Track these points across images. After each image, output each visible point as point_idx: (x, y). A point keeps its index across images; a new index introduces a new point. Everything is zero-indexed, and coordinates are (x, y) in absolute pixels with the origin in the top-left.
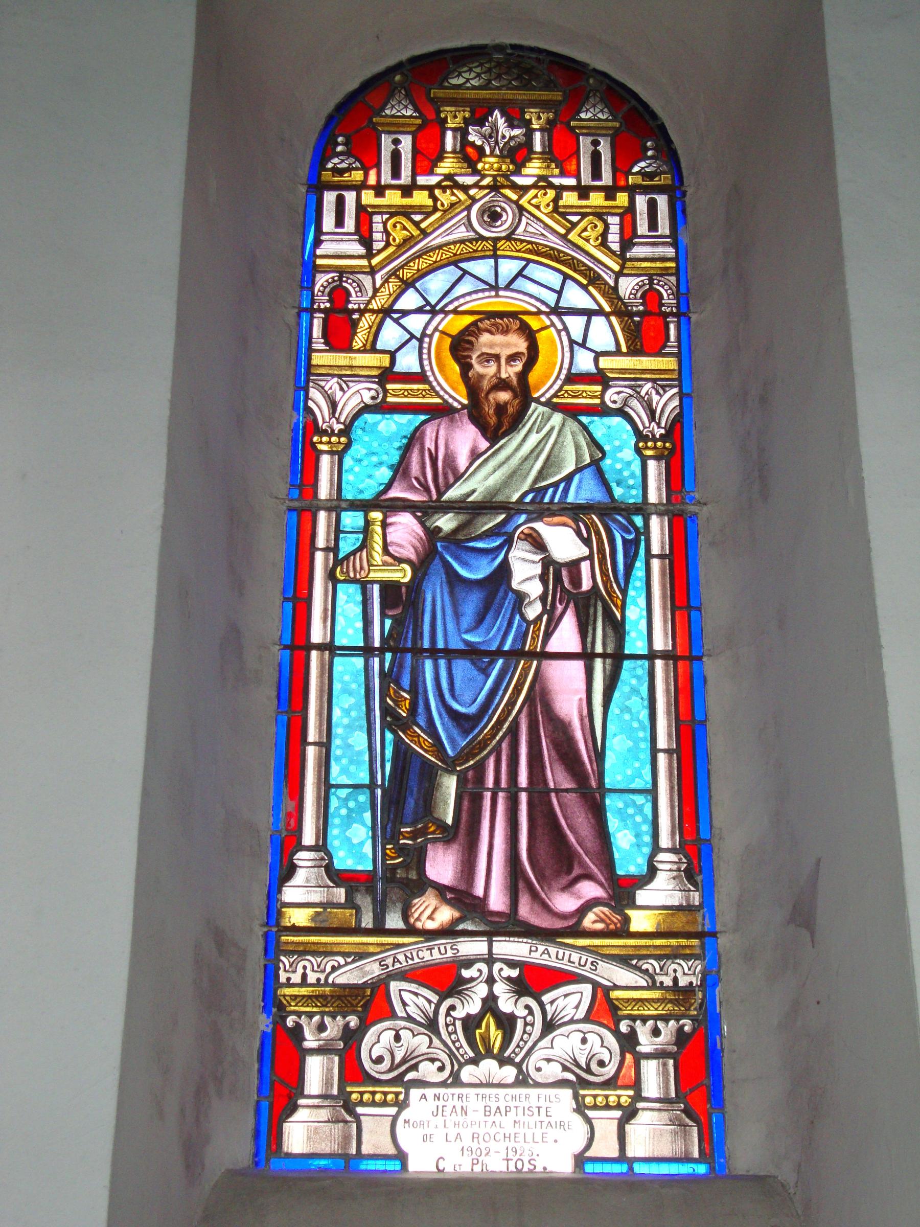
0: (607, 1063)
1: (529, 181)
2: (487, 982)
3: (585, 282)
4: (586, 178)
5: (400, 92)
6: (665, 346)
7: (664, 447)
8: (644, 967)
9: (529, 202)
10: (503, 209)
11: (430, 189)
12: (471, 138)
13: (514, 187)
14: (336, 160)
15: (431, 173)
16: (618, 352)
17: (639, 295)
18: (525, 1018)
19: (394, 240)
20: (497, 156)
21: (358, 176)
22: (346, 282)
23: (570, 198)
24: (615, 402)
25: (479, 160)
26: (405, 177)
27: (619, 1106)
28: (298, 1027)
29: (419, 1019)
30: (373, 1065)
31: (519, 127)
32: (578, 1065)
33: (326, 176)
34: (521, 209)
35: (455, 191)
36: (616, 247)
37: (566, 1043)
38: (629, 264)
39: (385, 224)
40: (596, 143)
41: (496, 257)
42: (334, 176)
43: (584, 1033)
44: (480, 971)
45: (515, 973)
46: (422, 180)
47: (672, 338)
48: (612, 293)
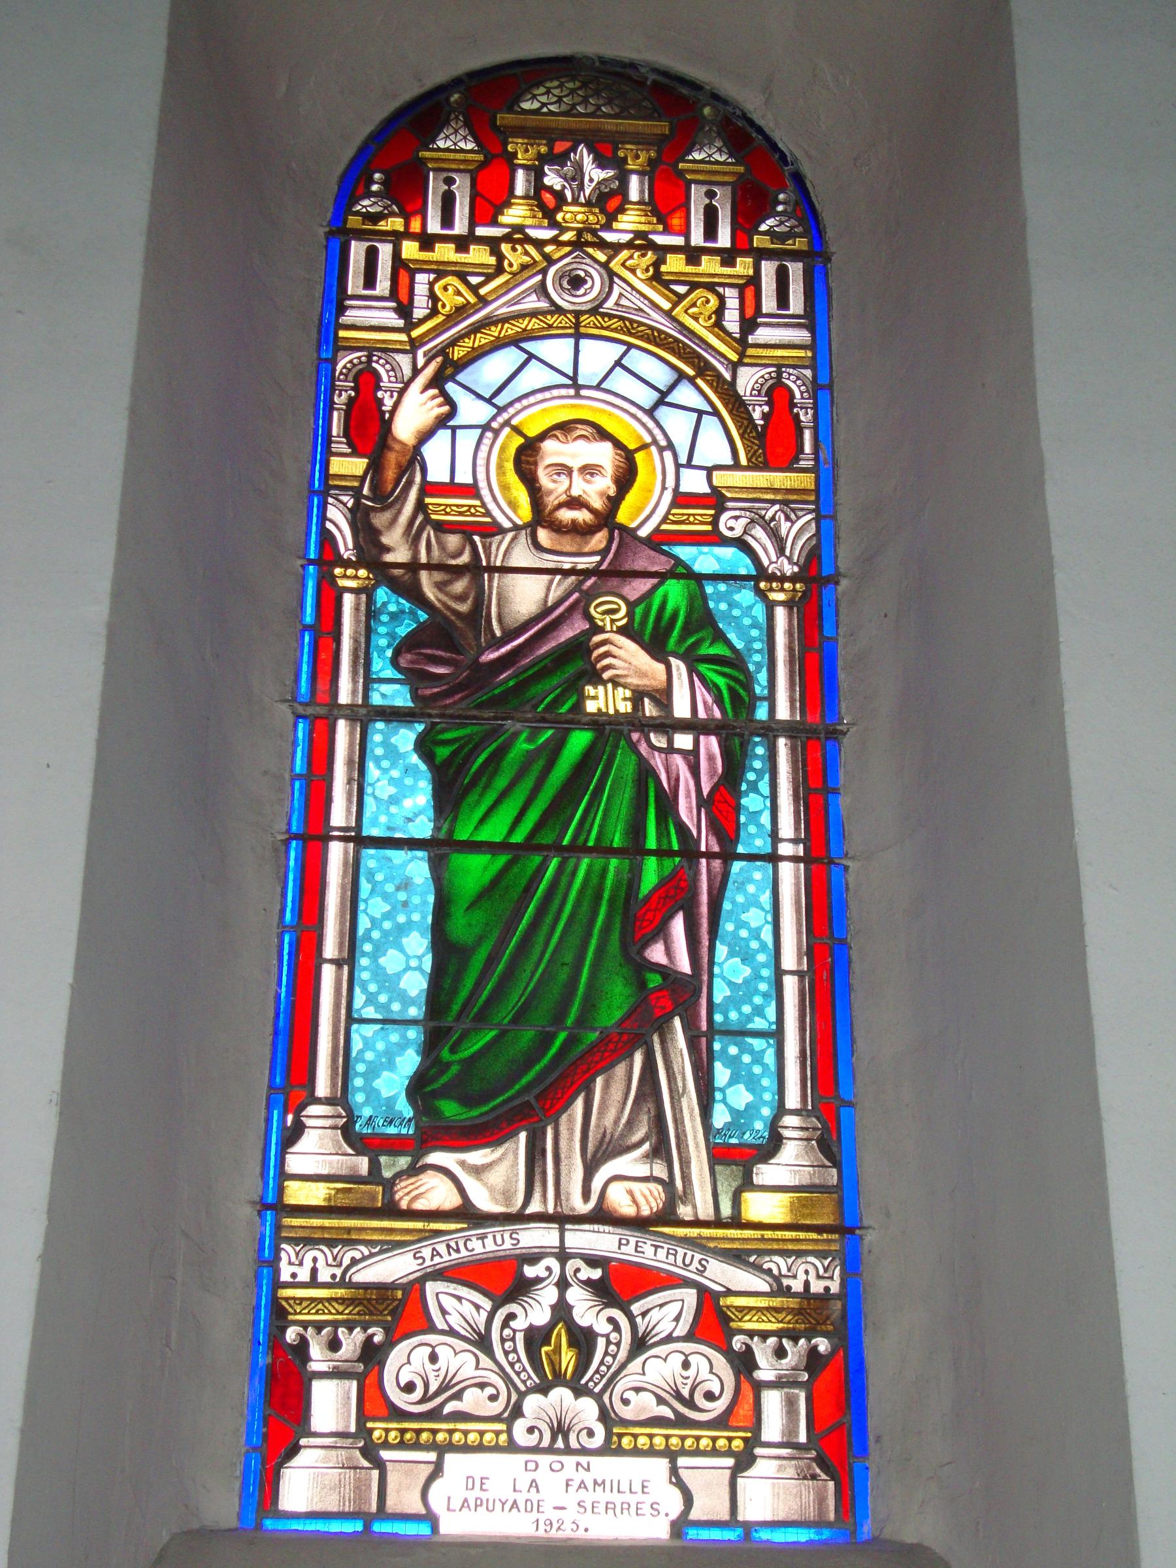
0: (717, 1394)
1: (625, 238)
2: (557, 1284)
3: (691, 372)
4: (697, 238)
5: (457, 118)
6: (798, 460)
8: (765, 1266)
9: (623, 265)
11: (493, 244)
12: (547, 181)
13: (602, 245)
14: (366, 202)
15: (494, 223)
16: (736, 466)
17: (763, 392)
18: (607, 1336)
20: (582, 205)
21: (397, 224)
22: (377, 362)
23: (675, 264)
24: (731, 529)
25: (558, 209)
26: (460, 227)
27: (729, 1453)
28: (303, 1343)
29: (463, 1332)
32: (678, 1396)
33: (353, 222)
34: (612, 274)
37: (660, 1368)
38: (750, 352)
39: (431, 285)
40: (711, 195)
41: (578, 336)
42: (363, 224)
43: (686, 1356)
44: (548, 1269)
45: (596, 1274)
46: (481, 231)
47: (808, 448)
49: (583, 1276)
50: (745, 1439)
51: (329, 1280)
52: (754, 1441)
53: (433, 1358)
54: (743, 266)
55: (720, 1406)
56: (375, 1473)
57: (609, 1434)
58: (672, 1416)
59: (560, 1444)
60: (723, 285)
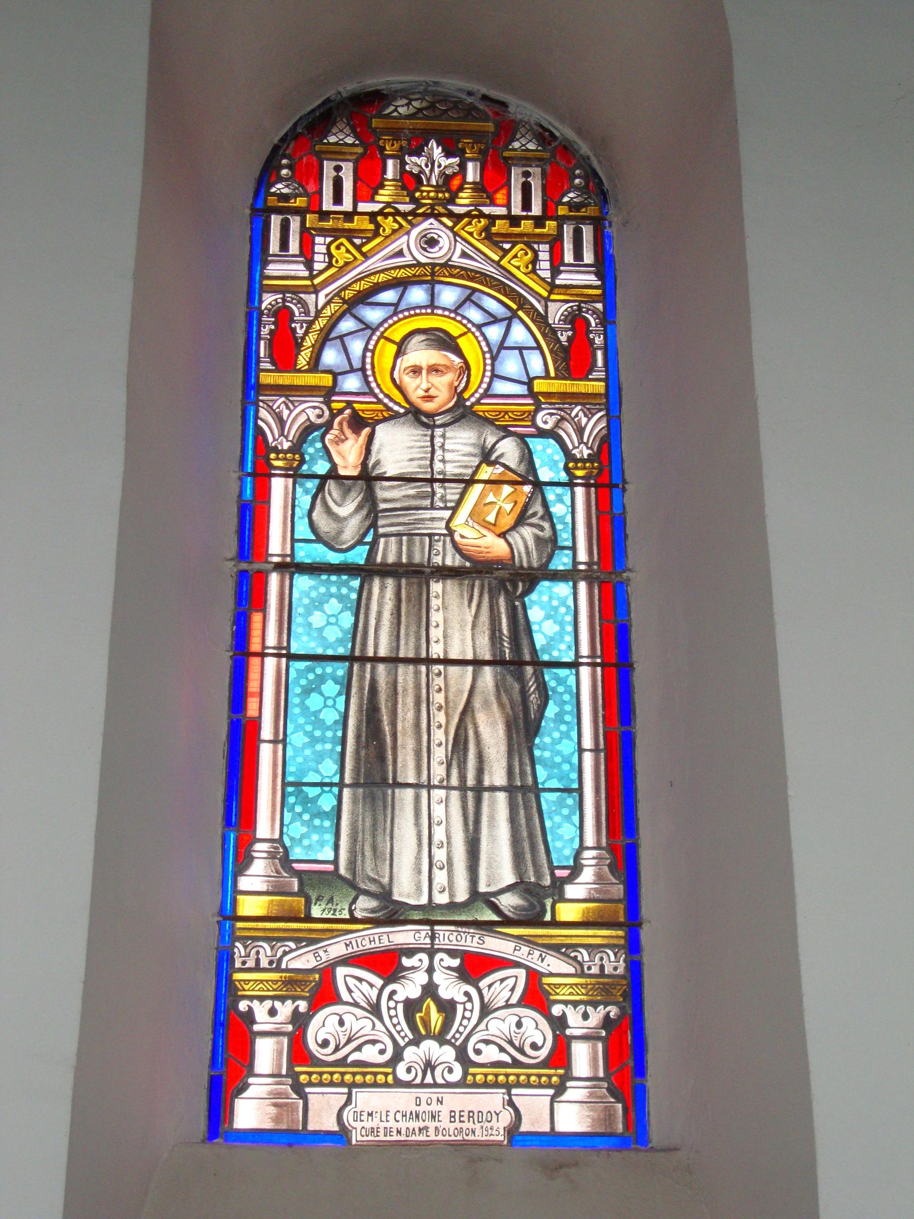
0: (540, 1044)
4: (517, 210)
5: (341, 120)
7: (593, 468)
8: (572, 955)
10: (439, 236)
11: (373, 216)
13: (450, 215)
14: (279, 186)
15: (372, 200)
16: (547, 376)
18: (464, 1003)
19: (337, 261)
20: (432, 186)
21: (300, 202)
26: (347, 205)
27: (549, 1086)
30: (319, 1049)
31: (454, 156)
35: (397, 218)
36: (546, 274)
37: (500, 1025)
40: (527, 174)
43: (520, 1018)
46: (363, 207)
47: (600, 362)
48: (541, 320)
49: (444, 964)
50: (560, 1076)
51: (268, 966)
52: (568, 1076)
53: (341, 1023)
54: (551, 226)
55: (543, 1053)
56: (301, 1101)
57: (465, 1074)
58: (509, 1060)
59: (429, 1079)
60: (538, 243)
